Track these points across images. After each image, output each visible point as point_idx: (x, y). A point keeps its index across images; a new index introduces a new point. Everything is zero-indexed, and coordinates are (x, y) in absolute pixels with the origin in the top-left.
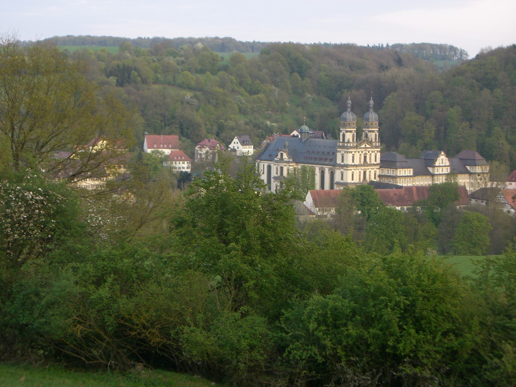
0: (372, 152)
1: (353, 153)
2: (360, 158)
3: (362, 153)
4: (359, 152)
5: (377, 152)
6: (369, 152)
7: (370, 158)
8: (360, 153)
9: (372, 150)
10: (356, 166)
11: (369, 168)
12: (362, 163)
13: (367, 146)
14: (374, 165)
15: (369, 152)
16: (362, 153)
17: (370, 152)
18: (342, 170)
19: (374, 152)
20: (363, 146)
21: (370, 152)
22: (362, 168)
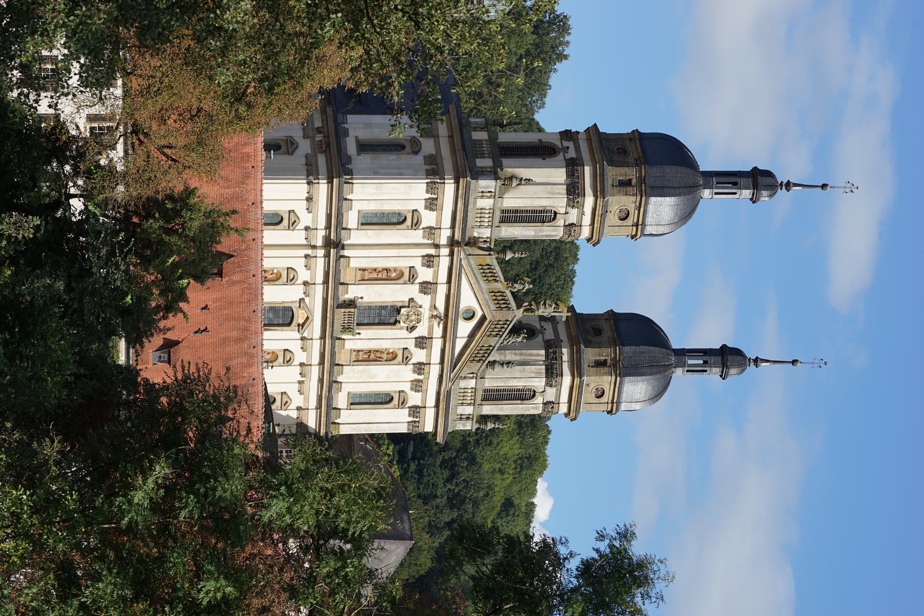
0: (420, 368)
1: (428, 218)
2: (386, 276)
3: (427, 288)
4: (429, 261)
5: (415, 411)
6: (422, 342)
7: (371, 357)
8: (425, 274)
9: (435, 371)
10: (334, 245)
11: (316, 345)
12: (352, 292)
13: (465, 328)
14: (329, 385)
15: (422, 342)
16: (427, 288)
17: (419, 355)
18: (305, 147)
19: (417, 386)
20: (468, 299)
21: (419, 355)
22: (319, 290)
